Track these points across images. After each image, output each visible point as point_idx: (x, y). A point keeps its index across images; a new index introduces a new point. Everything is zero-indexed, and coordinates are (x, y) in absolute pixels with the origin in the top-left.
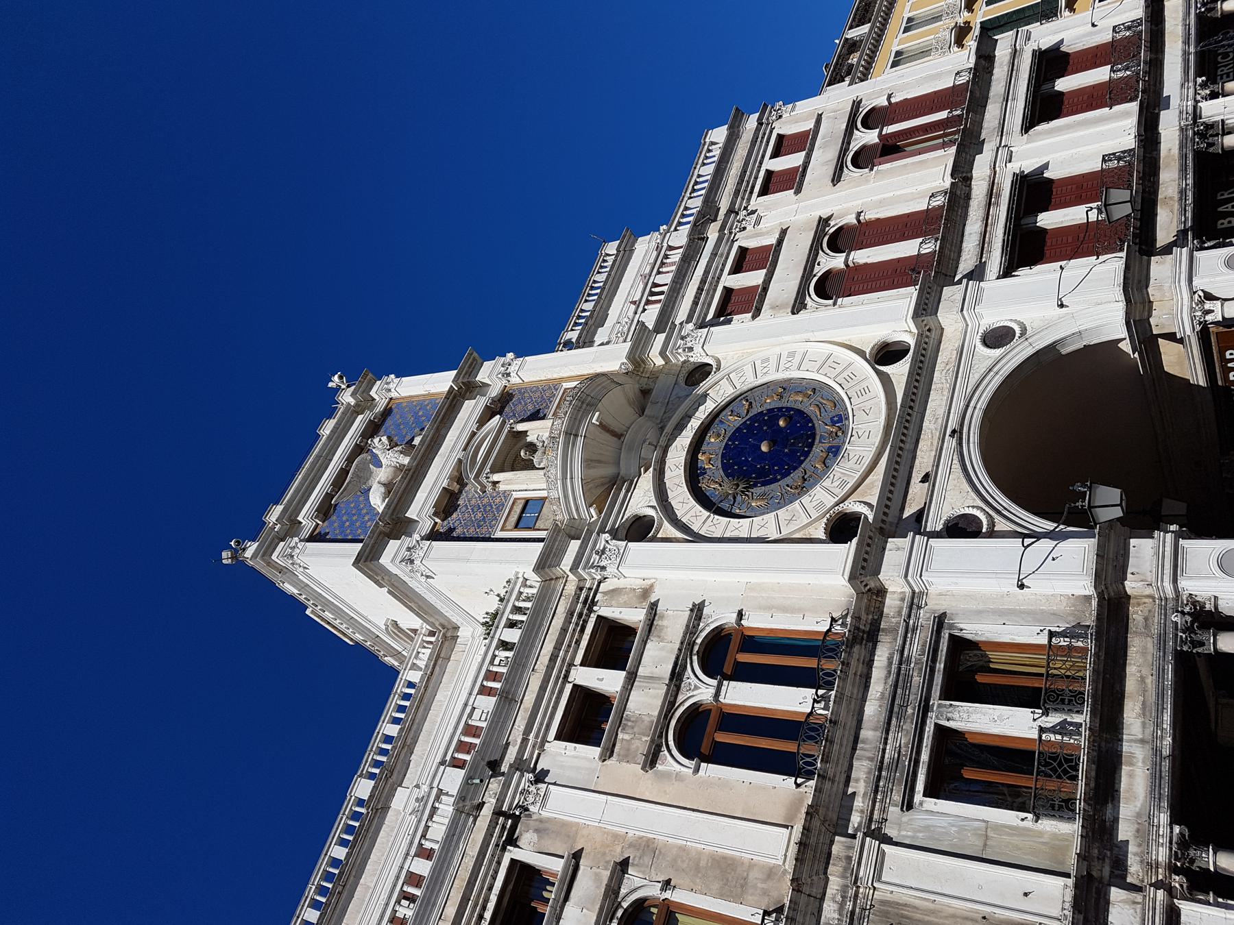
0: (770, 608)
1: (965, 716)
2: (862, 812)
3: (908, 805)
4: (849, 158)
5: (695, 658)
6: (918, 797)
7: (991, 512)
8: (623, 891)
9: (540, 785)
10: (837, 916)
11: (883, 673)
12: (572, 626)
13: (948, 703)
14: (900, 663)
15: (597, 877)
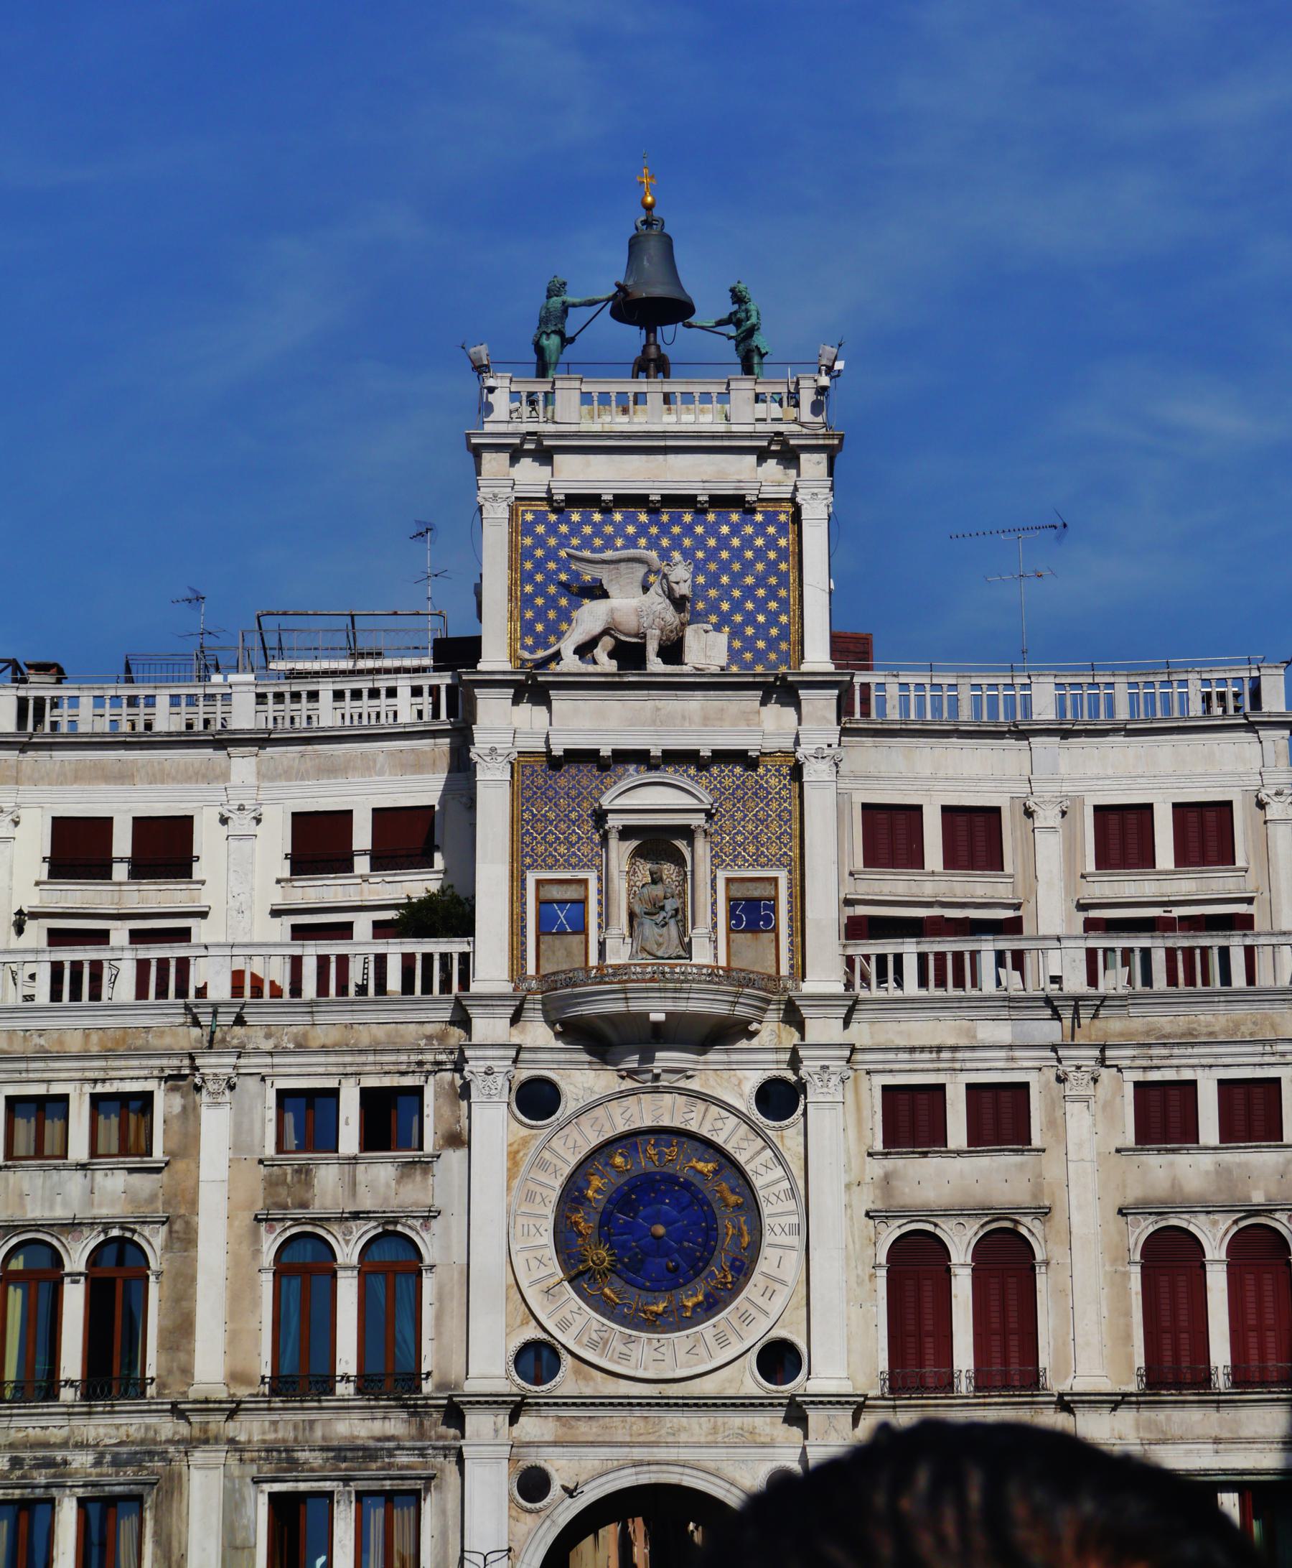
0: (440, 1298)
1: (343, 1515)
2: (249, 1442)
3: (257, 1481)
4: (1174, 1221)
5: (380, 1230)
6: (268, 1488)
7: (548, 1512)
8: (147, 1231)
9: (227, 1092)
10: (163, 1438)
11: (377, 1433)
12: (404, 1058)
13: (353, 1499)
14: (388, 1449)
15: (152, 1198)
